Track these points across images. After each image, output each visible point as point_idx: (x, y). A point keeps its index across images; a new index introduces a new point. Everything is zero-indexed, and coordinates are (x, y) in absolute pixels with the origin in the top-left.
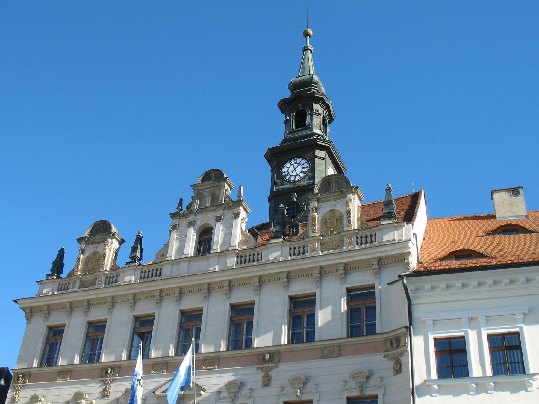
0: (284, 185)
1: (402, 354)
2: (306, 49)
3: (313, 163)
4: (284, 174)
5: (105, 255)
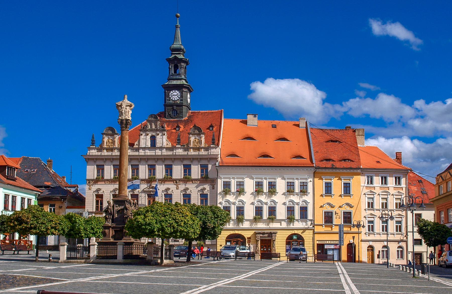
1: (215, 184)
2: (177, 27)
3: (182, 93)
4: (170, 96)
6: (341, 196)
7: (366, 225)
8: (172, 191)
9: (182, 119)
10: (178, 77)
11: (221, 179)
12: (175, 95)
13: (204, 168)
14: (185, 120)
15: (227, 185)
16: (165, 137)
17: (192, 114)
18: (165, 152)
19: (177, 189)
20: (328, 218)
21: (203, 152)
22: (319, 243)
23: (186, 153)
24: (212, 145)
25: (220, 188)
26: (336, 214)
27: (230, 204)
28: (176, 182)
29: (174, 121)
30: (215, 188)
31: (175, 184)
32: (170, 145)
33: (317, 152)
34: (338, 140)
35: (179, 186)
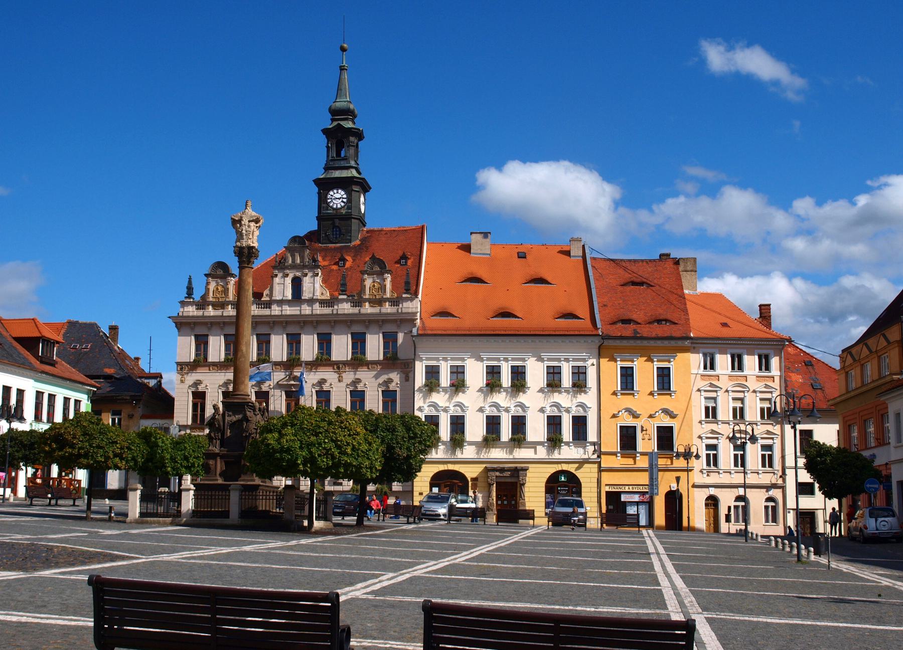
0: (328, 210)
1: (410, 372)
4: (329, 201)
5: (228, 289)
6: (651, 394)
7: (703, 453)
8: (331, 385)
9: (349, 244)
10: (343, 164)
11: (421, 360)
12: (337, 198)
13: (390, 340)
14: (354, 247)
15: (433, 373)
16: (319, 280)
17: (369, 235)
18: (318, 309)
19: (339, 381)
20: (628, 438)
21: (388, 308)
22: (610, 490)
23: (356, 310)
24: (405, 293)
25: (420, 378)
26: (642, 430)
27: (437, 410)
28: (338, 368)
29: (336, 249)
30: (411, 379)
31: (335, 372)
32: (327, 296)
33: (605, 305)
34: (645, 280)
35: (344, 375)
